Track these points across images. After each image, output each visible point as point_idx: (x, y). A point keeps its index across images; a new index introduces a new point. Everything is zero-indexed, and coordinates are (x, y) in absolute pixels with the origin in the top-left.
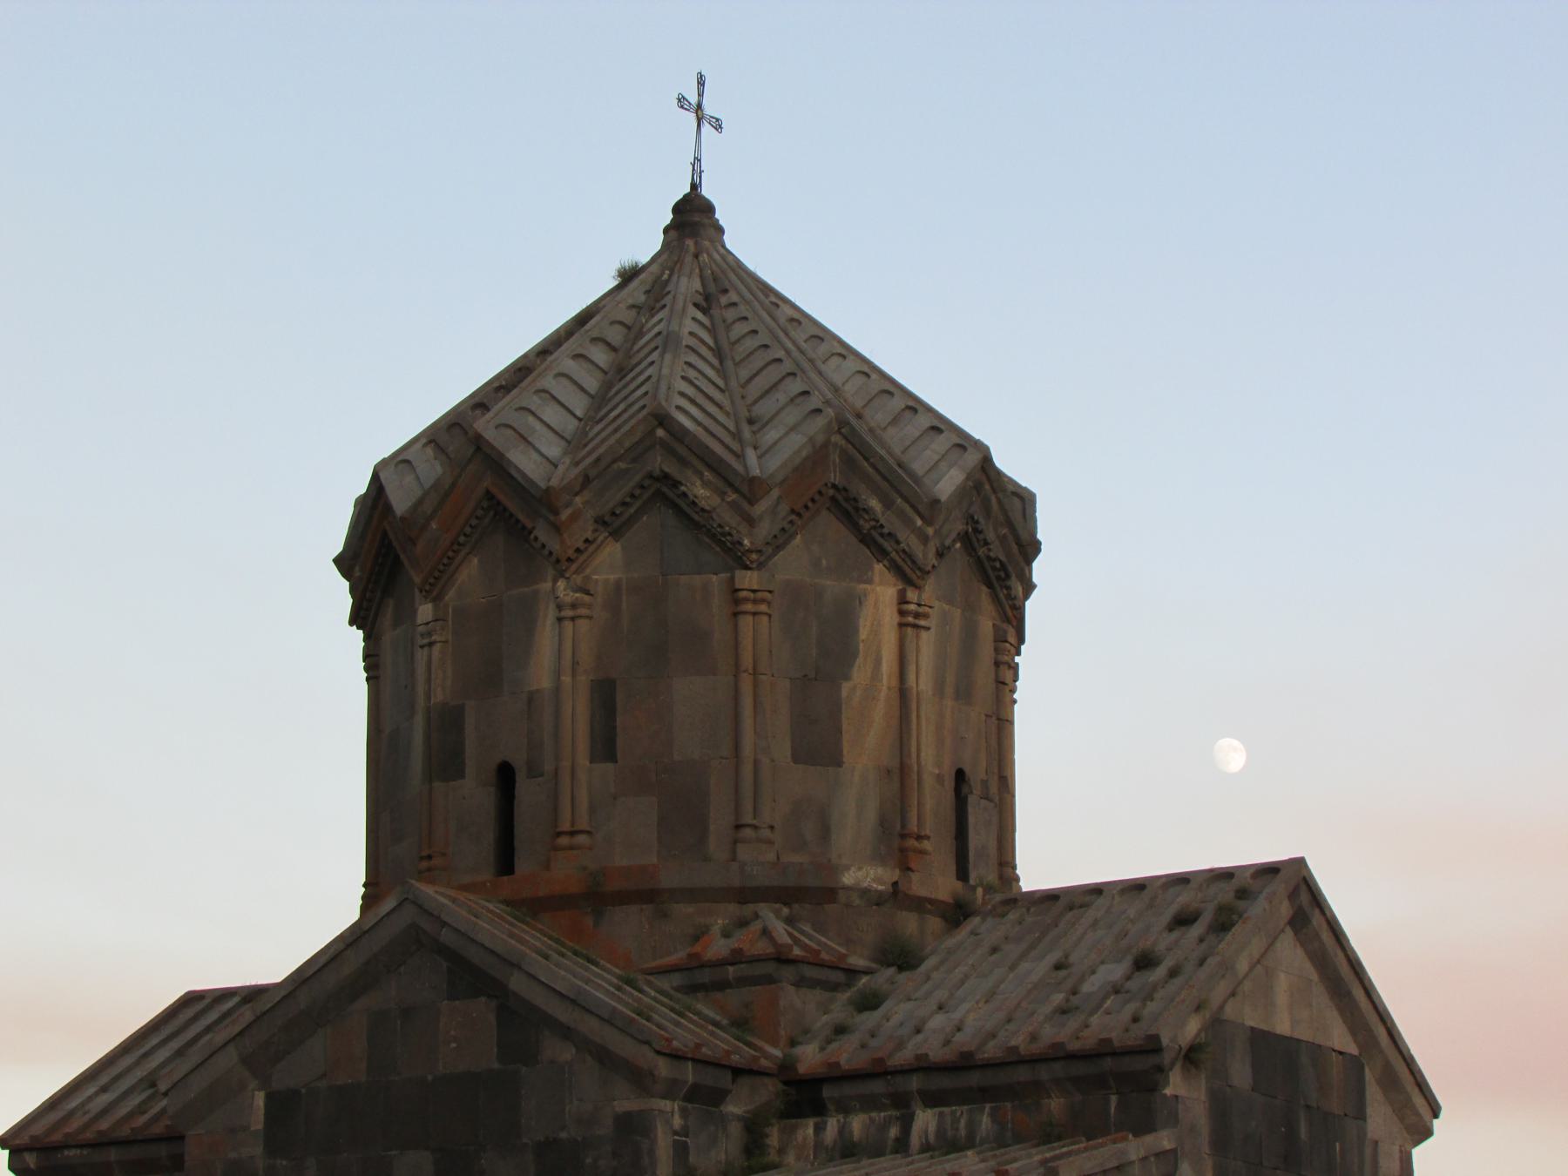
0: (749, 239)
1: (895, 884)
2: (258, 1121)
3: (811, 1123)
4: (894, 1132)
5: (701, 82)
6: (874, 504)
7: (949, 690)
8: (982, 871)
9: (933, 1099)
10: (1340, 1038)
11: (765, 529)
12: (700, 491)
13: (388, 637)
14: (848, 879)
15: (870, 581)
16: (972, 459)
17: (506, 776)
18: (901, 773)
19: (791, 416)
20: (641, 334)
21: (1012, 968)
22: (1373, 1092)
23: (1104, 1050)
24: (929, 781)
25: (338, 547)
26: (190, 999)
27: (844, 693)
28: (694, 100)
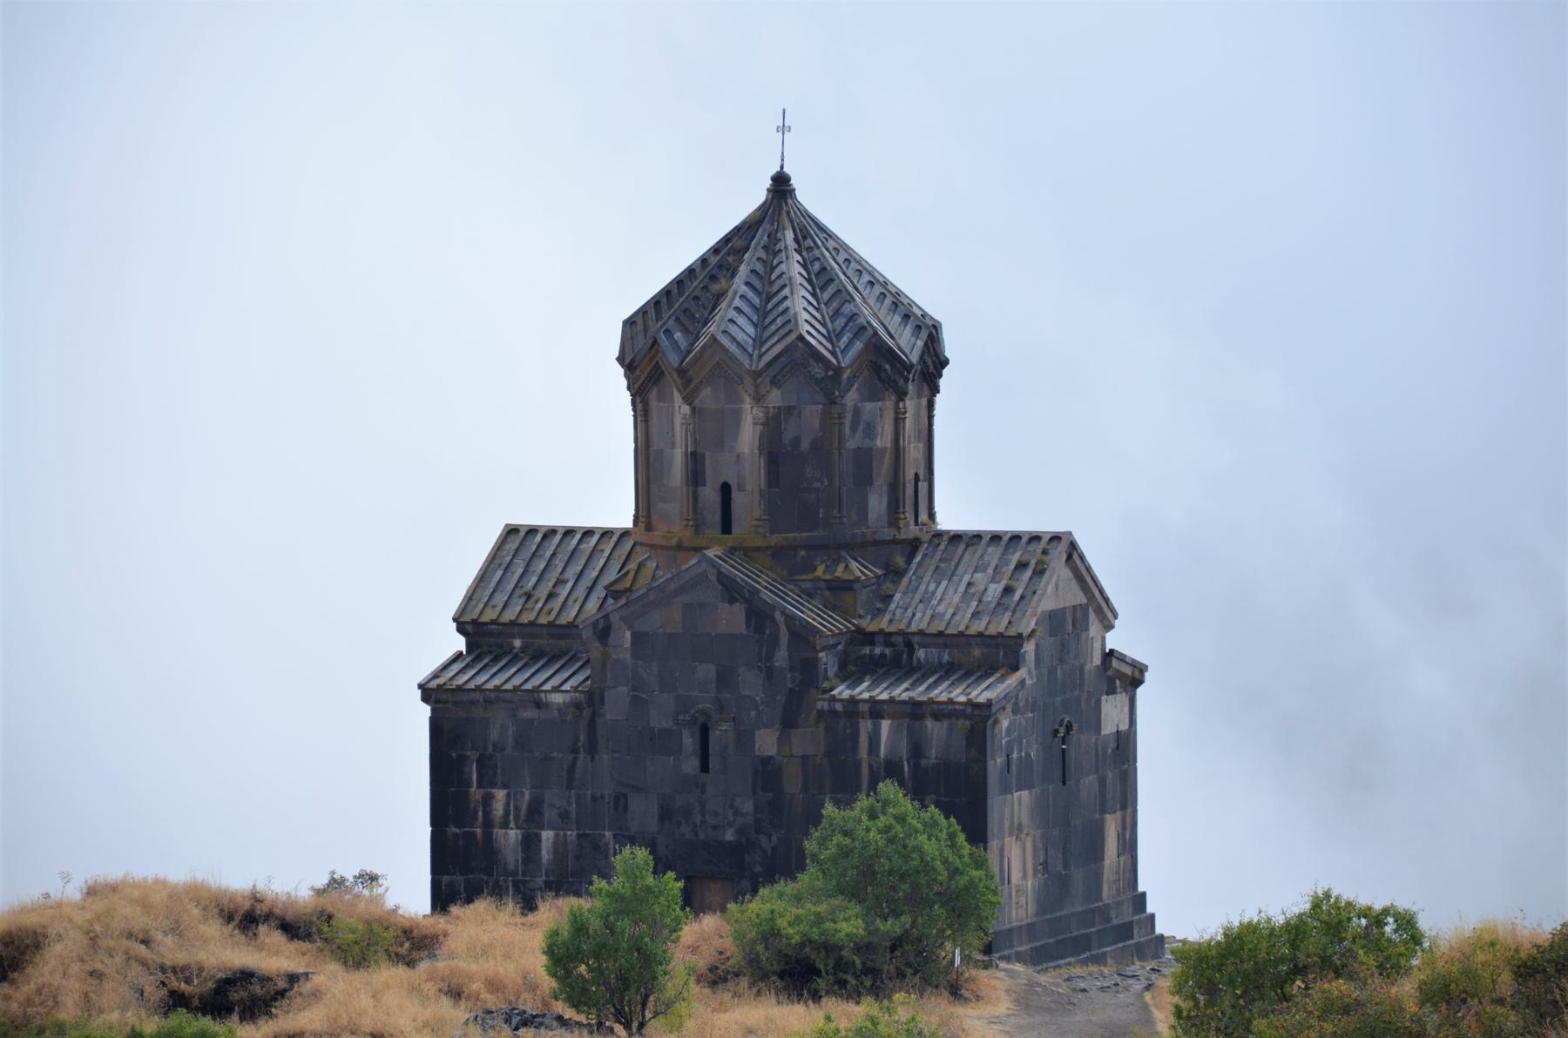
0: (807, 195)
8: (923, 517)
9: (922, 646)
10: (1081, 598)
13: (654, 404)
16: (924, 335)
17: (726, 489)
20: (773, 269)
22: (1092, 616)
23: (1001, 635)
26: (511, 531)
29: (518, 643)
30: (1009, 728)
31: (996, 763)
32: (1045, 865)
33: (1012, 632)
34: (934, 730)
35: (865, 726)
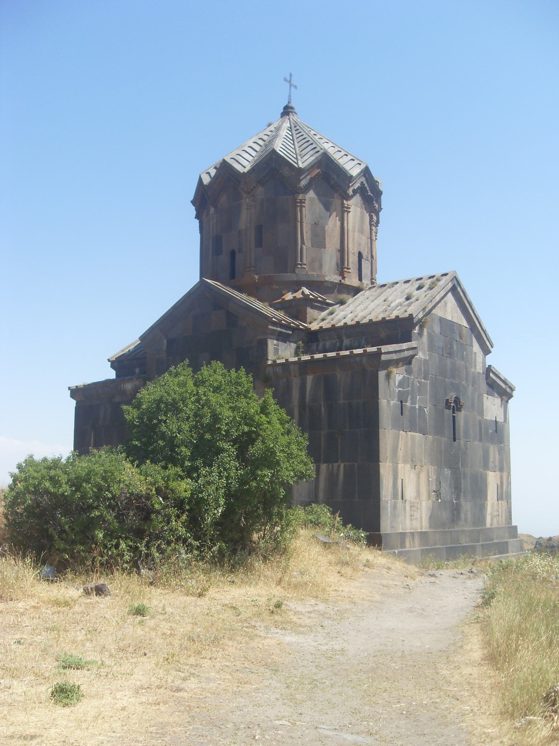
1: (340, 281)
2: (165, 347)
3: (315, 344)
4: (338, 345)
5: (291, 75)
6: (335, 177)
7: (357, 230)
9: (348, 337)
10: (464, 323)
11: (303, 183)
12: (286, 172)
14: (327, 279)
15: (334, 198)
17: (233, 254)
18: (342, 251)
19: (311, 153)
21: (372, 301)
24: (350, 255)
25: (192, 198)
27: (326, 229)
28: (289, 79)
29: (137, 370)
30: (401, 384)
31: (387, 405)
32: (438, 493)
33: (406, 315)
34: (342, 377)
35: (296, 382)
